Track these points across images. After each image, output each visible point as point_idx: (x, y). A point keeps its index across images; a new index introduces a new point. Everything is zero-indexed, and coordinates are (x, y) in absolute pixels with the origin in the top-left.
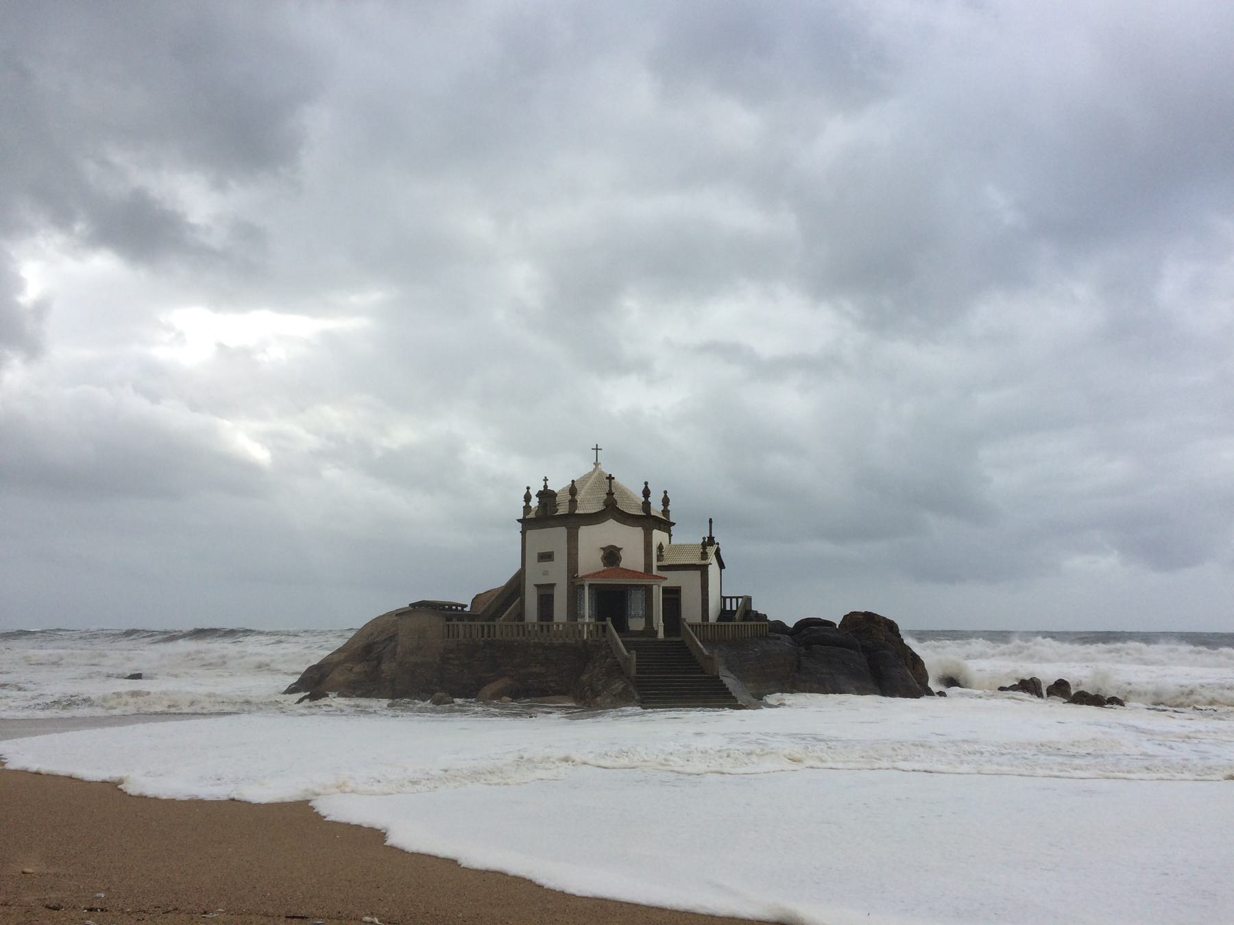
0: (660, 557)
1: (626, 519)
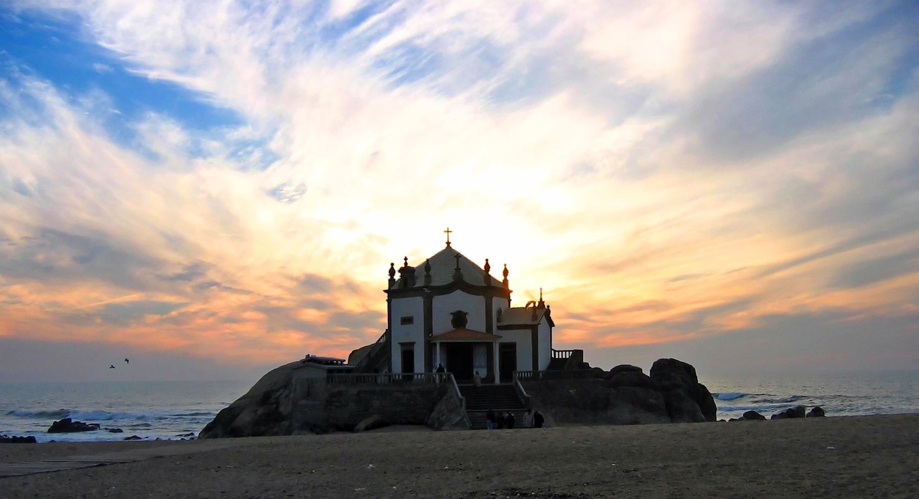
0: (498, 320)
1: (470, 289)
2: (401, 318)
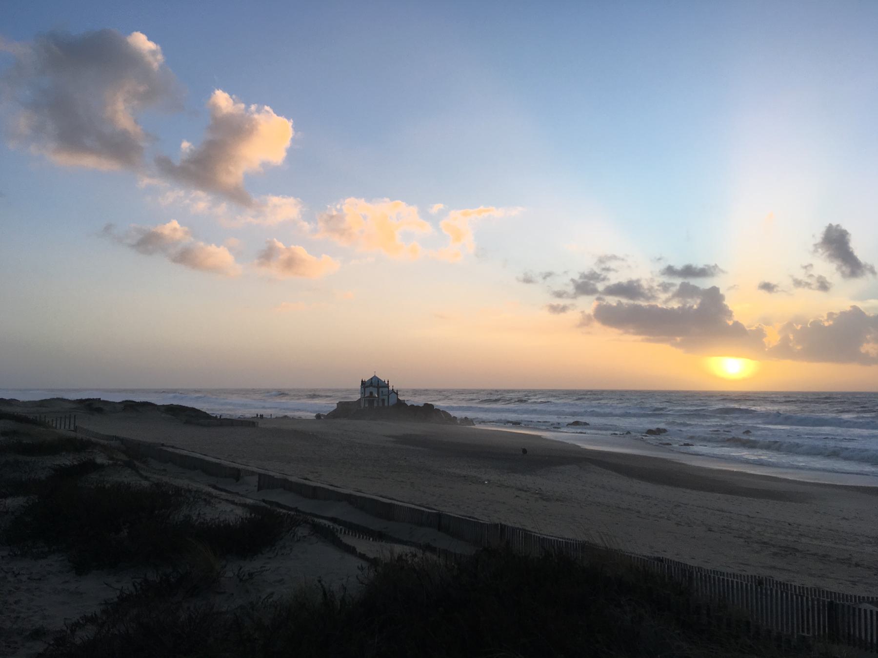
1: (374, 387)
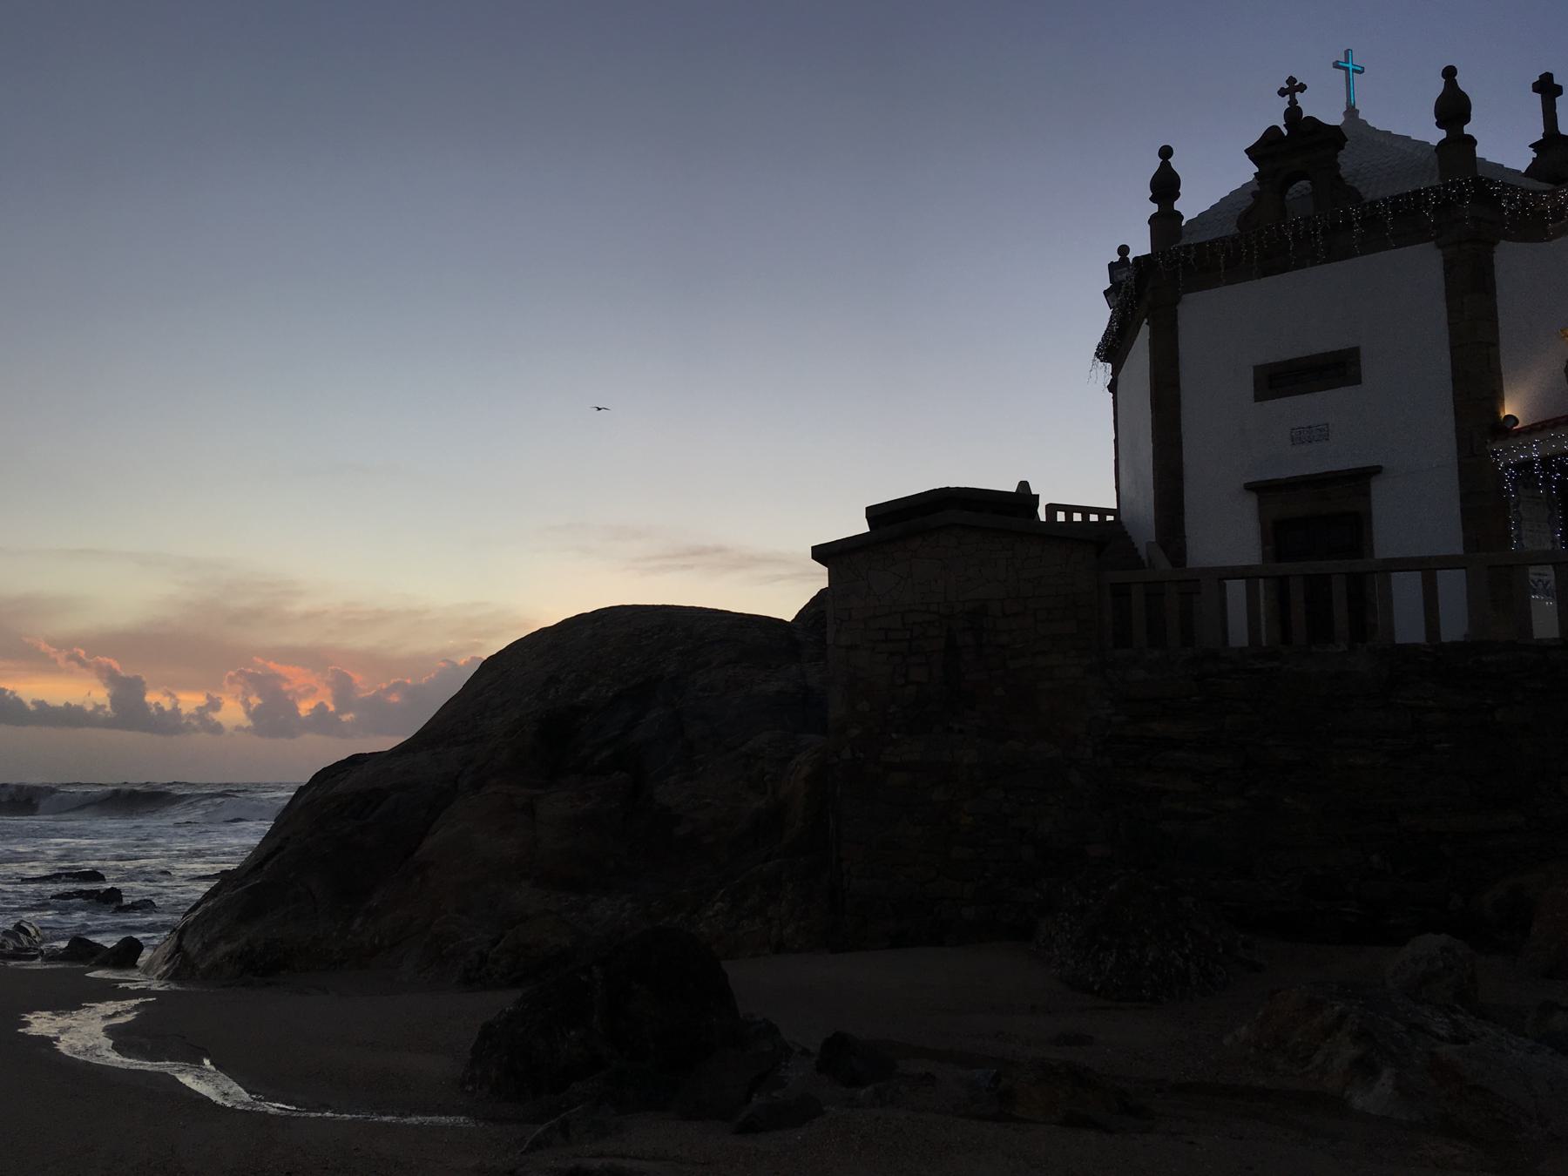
2: (1256, 368)
